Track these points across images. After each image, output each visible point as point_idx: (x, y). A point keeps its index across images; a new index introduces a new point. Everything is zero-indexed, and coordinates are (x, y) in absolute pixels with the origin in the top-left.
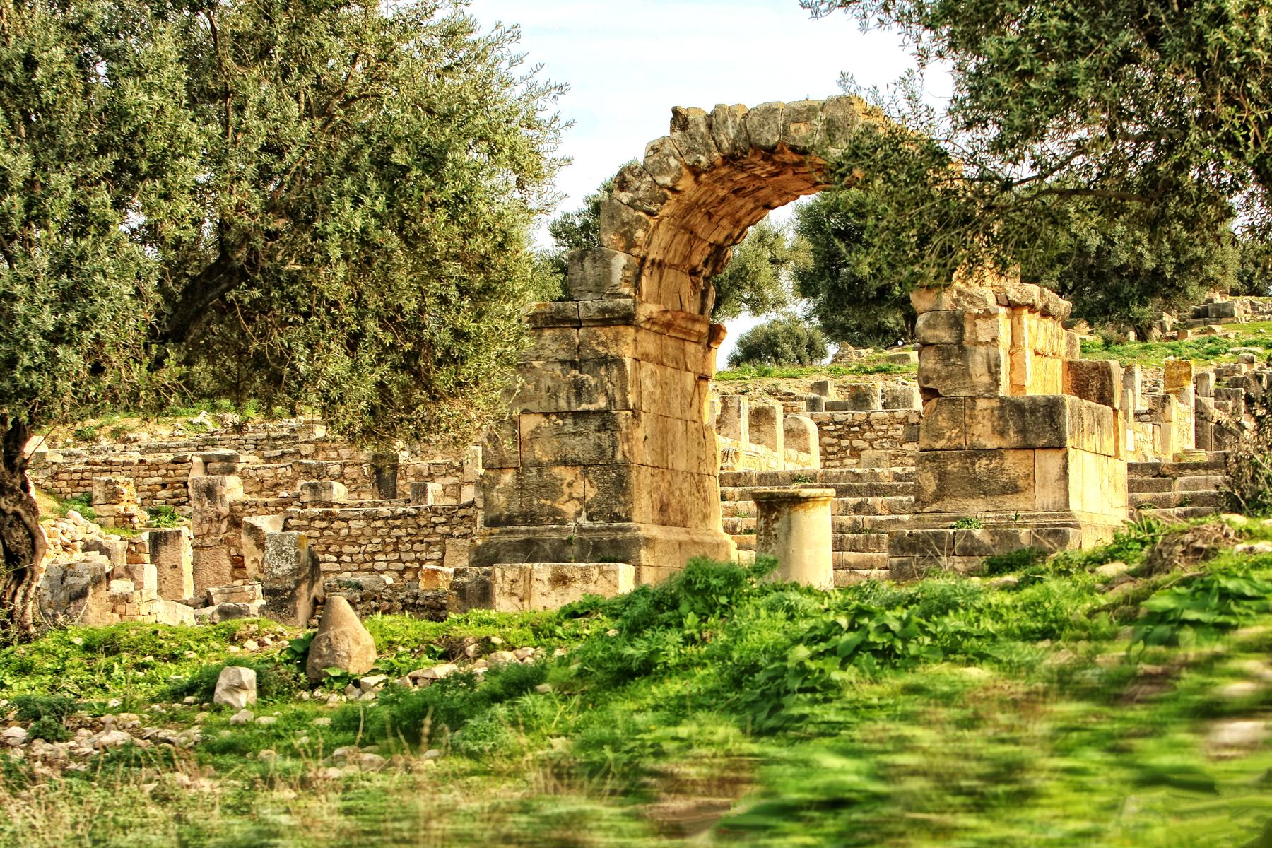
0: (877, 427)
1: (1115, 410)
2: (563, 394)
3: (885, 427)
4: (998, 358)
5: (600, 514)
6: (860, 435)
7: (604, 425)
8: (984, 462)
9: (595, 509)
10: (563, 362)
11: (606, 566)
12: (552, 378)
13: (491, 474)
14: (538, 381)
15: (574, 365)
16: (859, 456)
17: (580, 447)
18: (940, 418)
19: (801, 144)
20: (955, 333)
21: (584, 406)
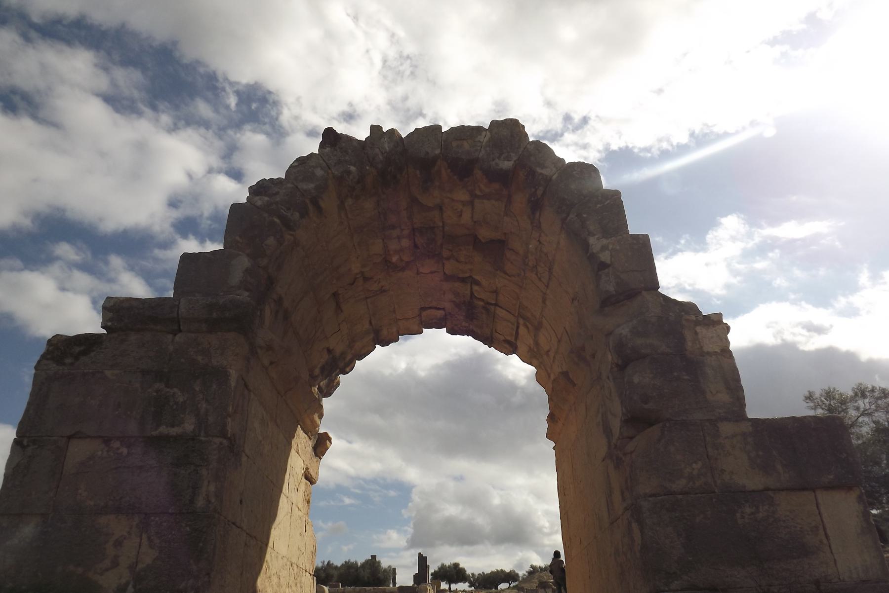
21: (163, 430)
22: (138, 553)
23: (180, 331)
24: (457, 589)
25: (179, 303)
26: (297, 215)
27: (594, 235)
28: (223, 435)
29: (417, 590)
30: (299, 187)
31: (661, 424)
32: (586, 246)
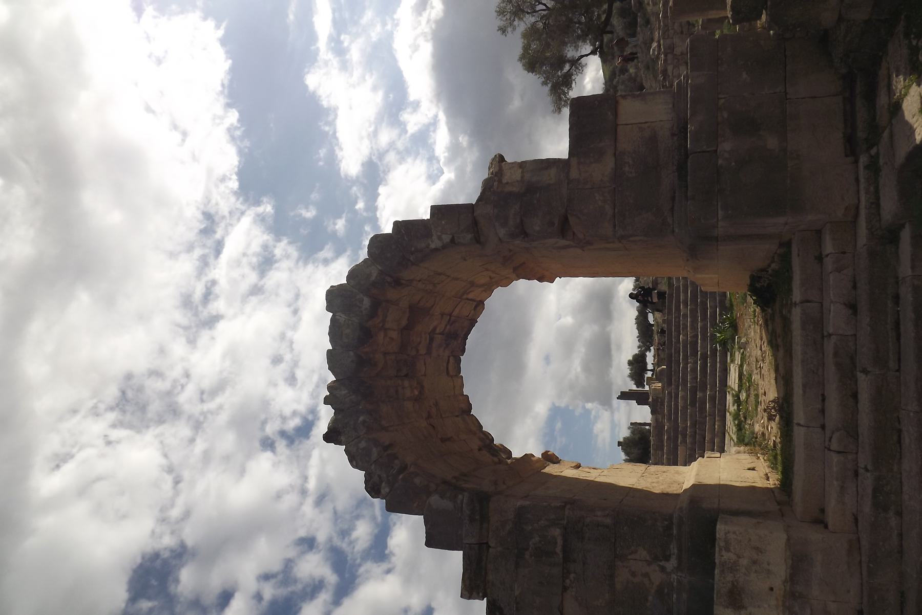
0: (657, 461)
8: (627, 169)
11: (720, 543)
21: (559, 549)
22: (640, 560)
23: (487, 543)
24: (652, 364)
25: (467, 544)
26: (396, 461)
27: (429, 245)
28: (563, 508)
29: (655, 398)
30: (375, 460)
31: (569, 216)
32: (436, 250)
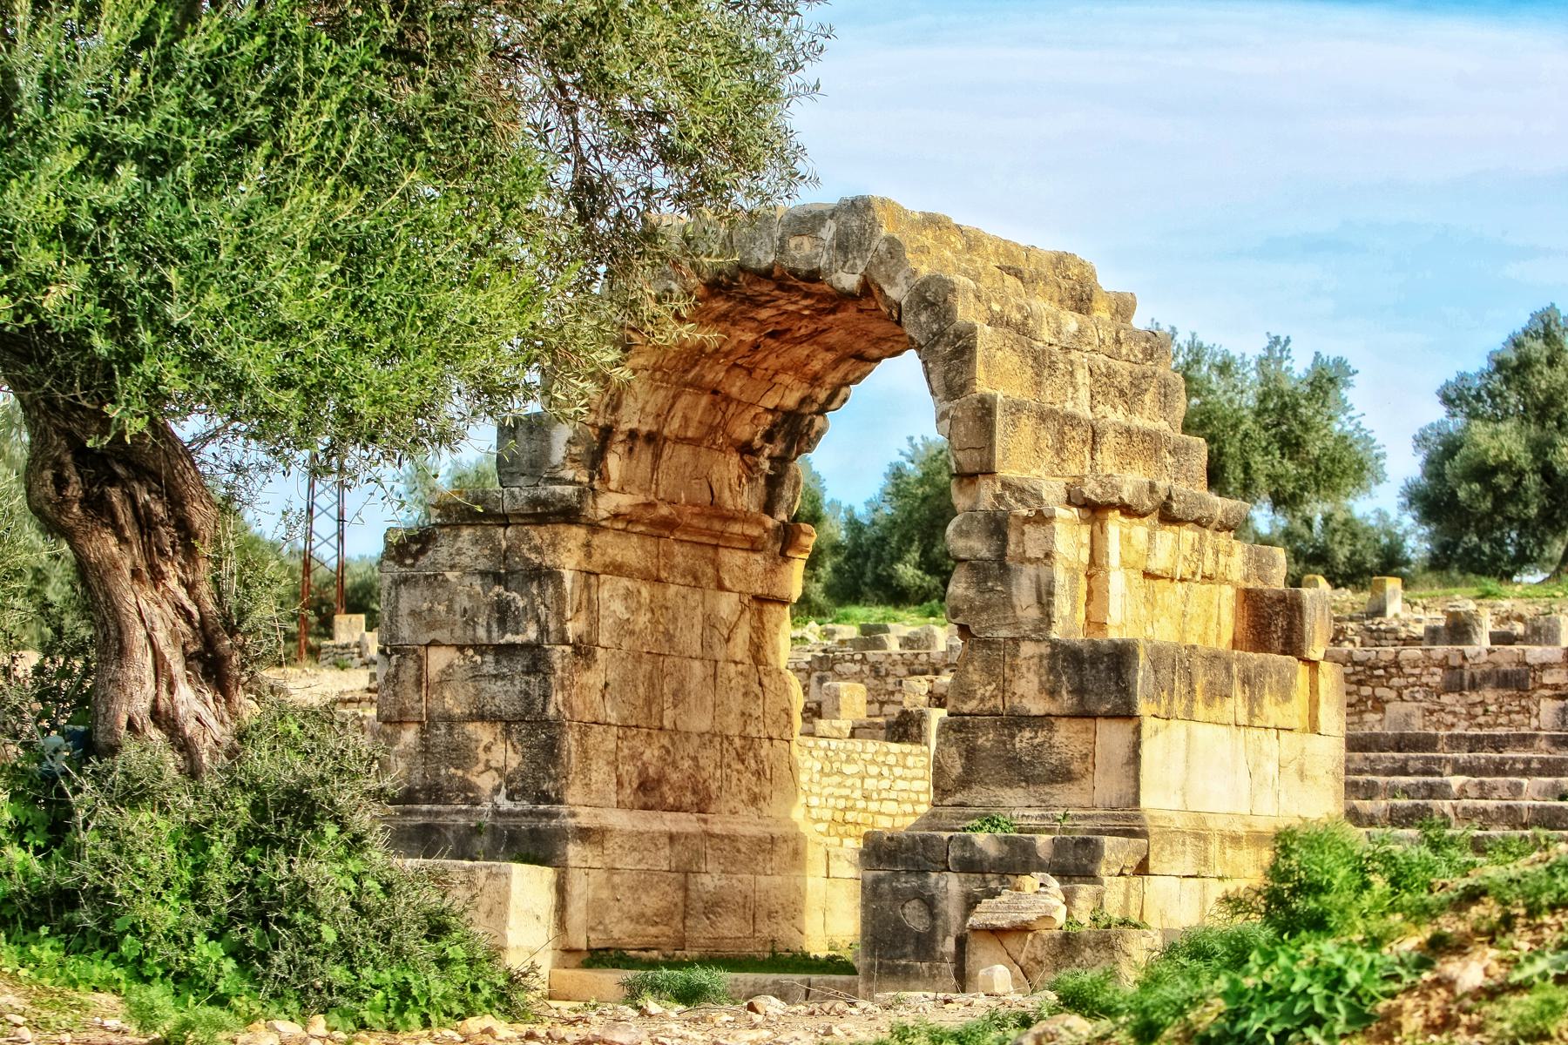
0: (1407, 670)
1: (1313, 665)
2: (482, 620)
3: (1417, 671)
4: (1051, 582)
5: (523, 792)
6: (1385, 681)
7: (535, 665)
8: (1027, 734)
9: (518, 784)
10: (483, 574)
12: (470, 596)
13: (389, 729)
14: (451, 601)
15: (498, 579)
16: (1383, 711)
17: (503, 694)
18: (970, 668)
19: (803, 267)
20: (995, 544)
21: (510, 638)
